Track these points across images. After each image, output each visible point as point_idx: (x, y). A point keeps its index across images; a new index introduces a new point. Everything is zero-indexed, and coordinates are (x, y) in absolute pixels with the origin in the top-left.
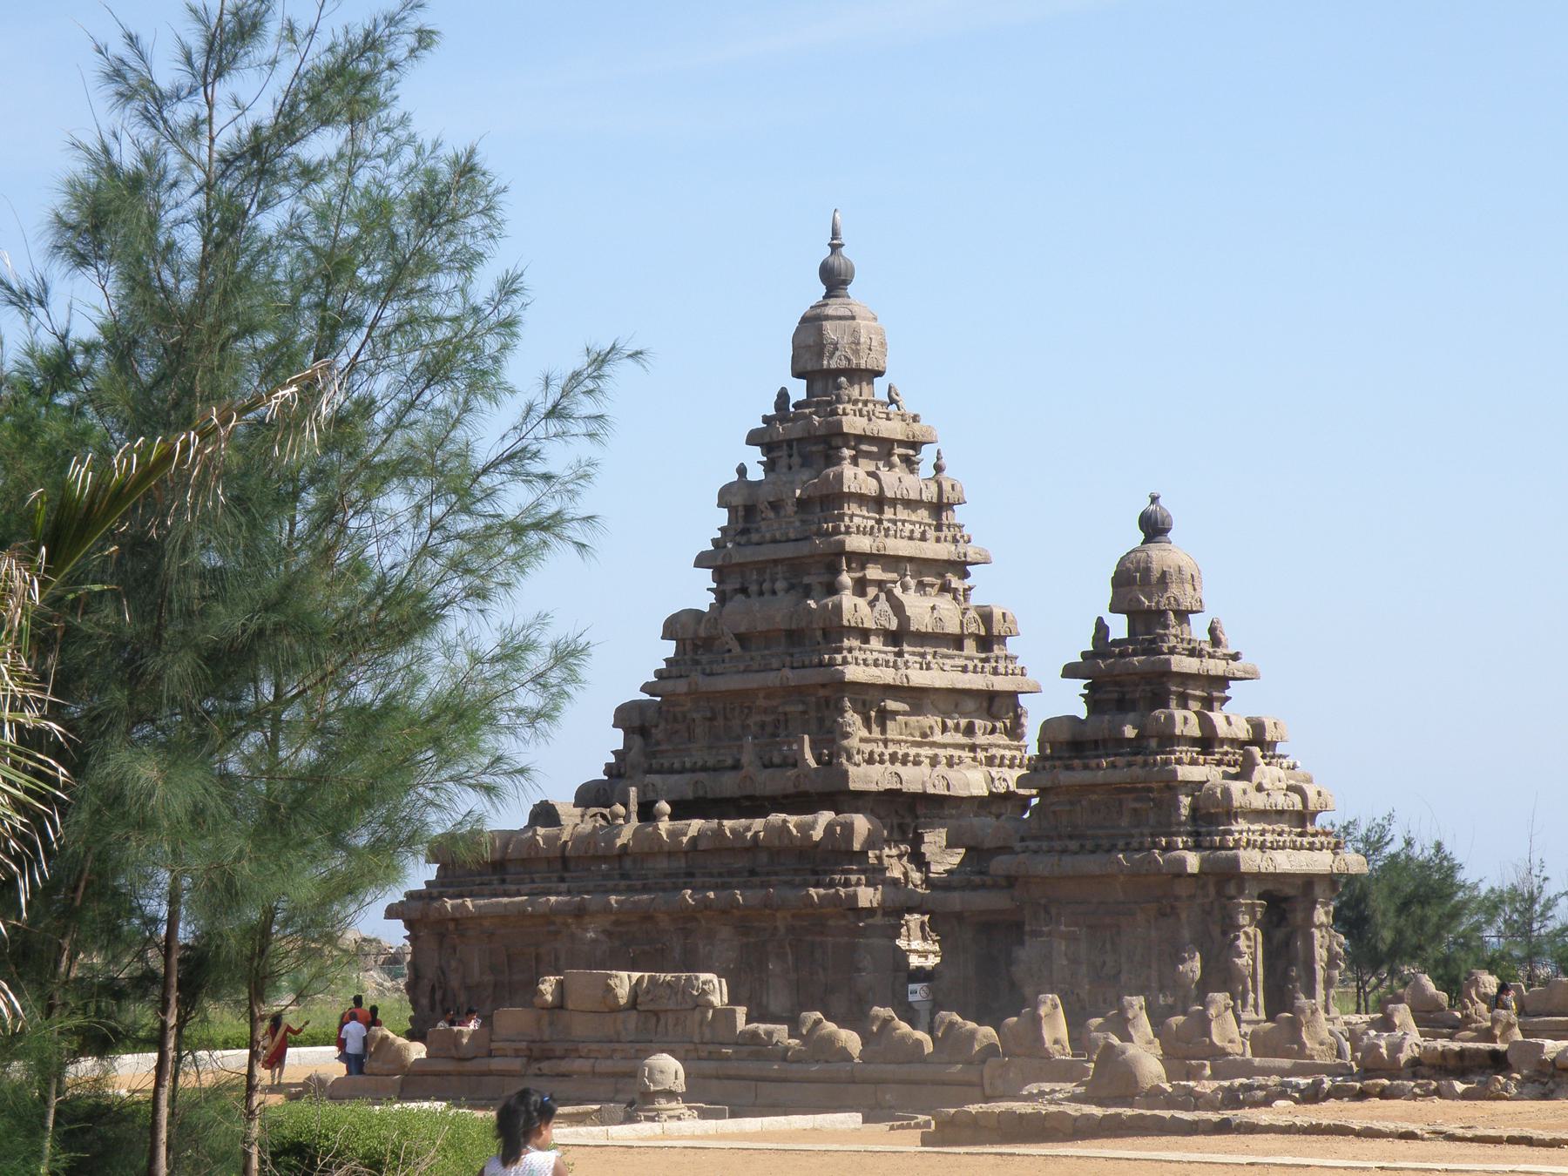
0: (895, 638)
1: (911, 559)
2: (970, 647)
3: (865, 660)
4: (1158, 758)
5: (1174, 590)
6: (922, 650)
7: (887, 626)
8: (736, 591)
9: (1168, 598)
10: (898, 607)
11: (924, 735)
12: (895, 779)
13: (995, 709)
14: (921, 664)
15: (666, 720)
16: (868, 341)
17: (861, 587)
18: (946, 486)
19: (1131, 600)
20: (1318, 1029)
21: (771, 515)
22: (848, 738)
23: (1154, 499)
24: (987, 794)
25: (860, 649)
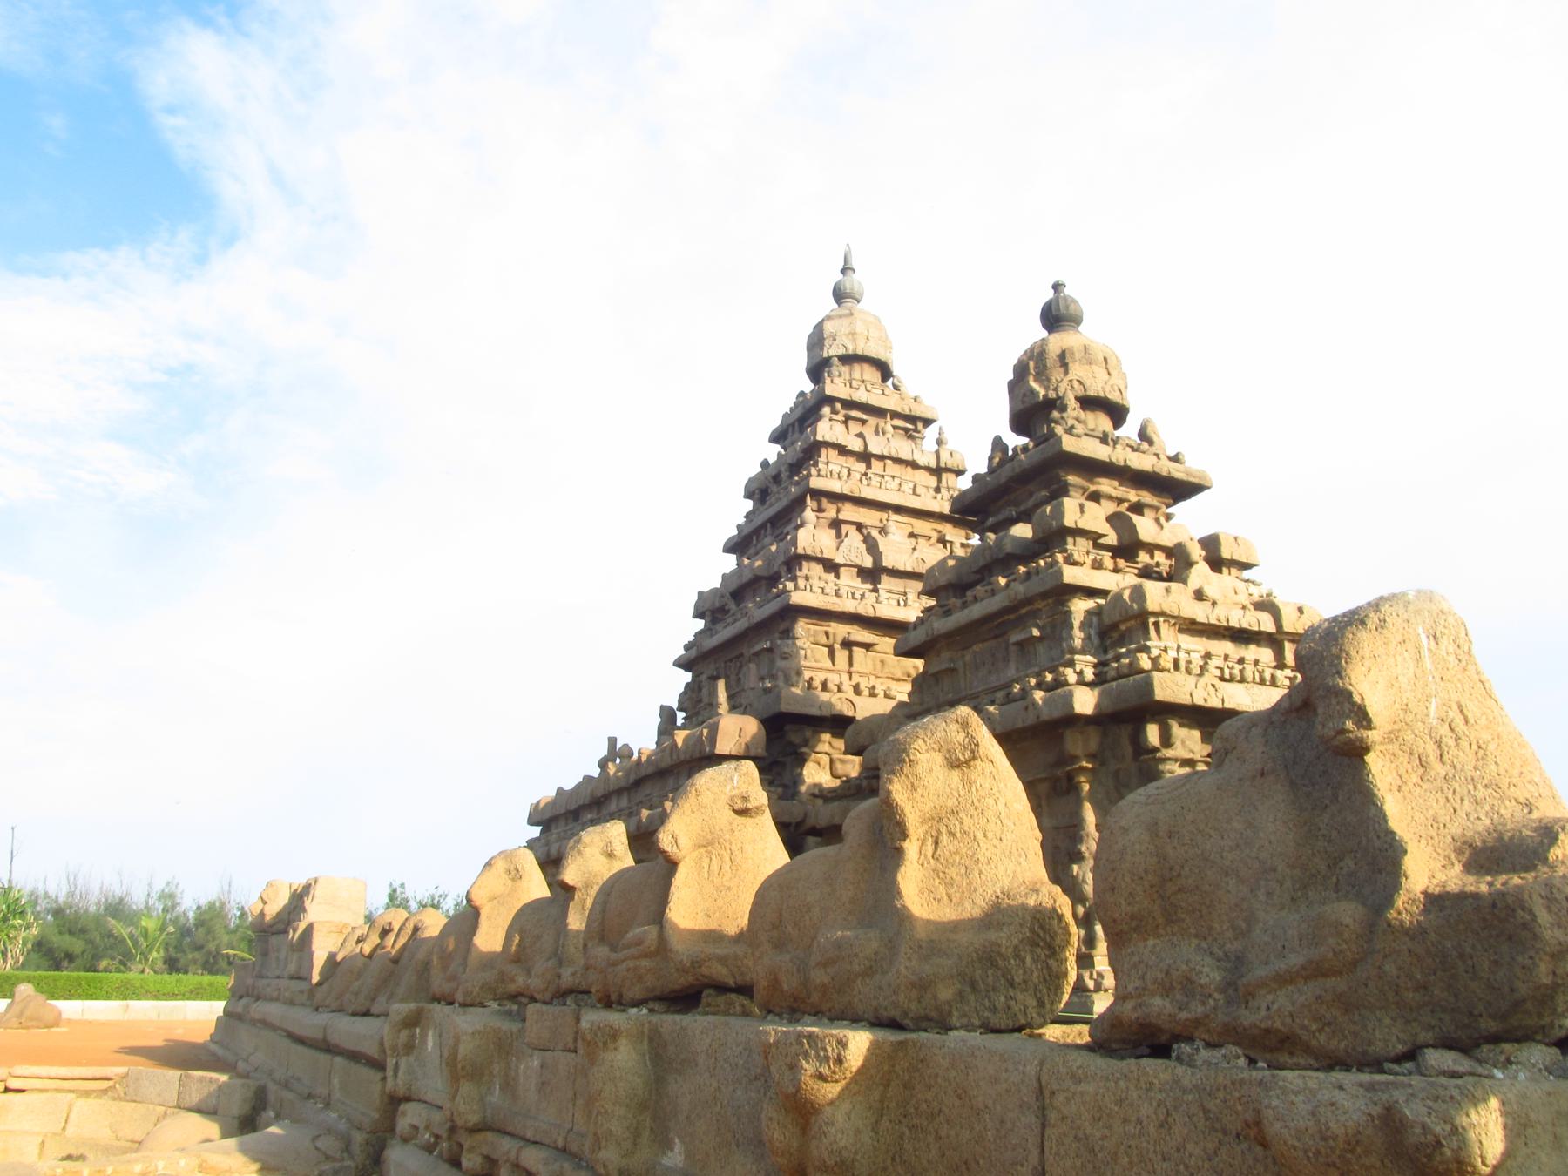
0: (872, 575)
1: (899, 509)
5: (1076, 371)
7: (859, 563)
9: (1071, 381)
10: (872, 547)
14: (899, 602)
15: (693, 691)
16: (866, 332)
17: (836, 524)
18: (945, 457)
19: (1024, 395)
20: (985, 851)
21: (774, 488)
22: (785, 658)
23: (1057, 287)
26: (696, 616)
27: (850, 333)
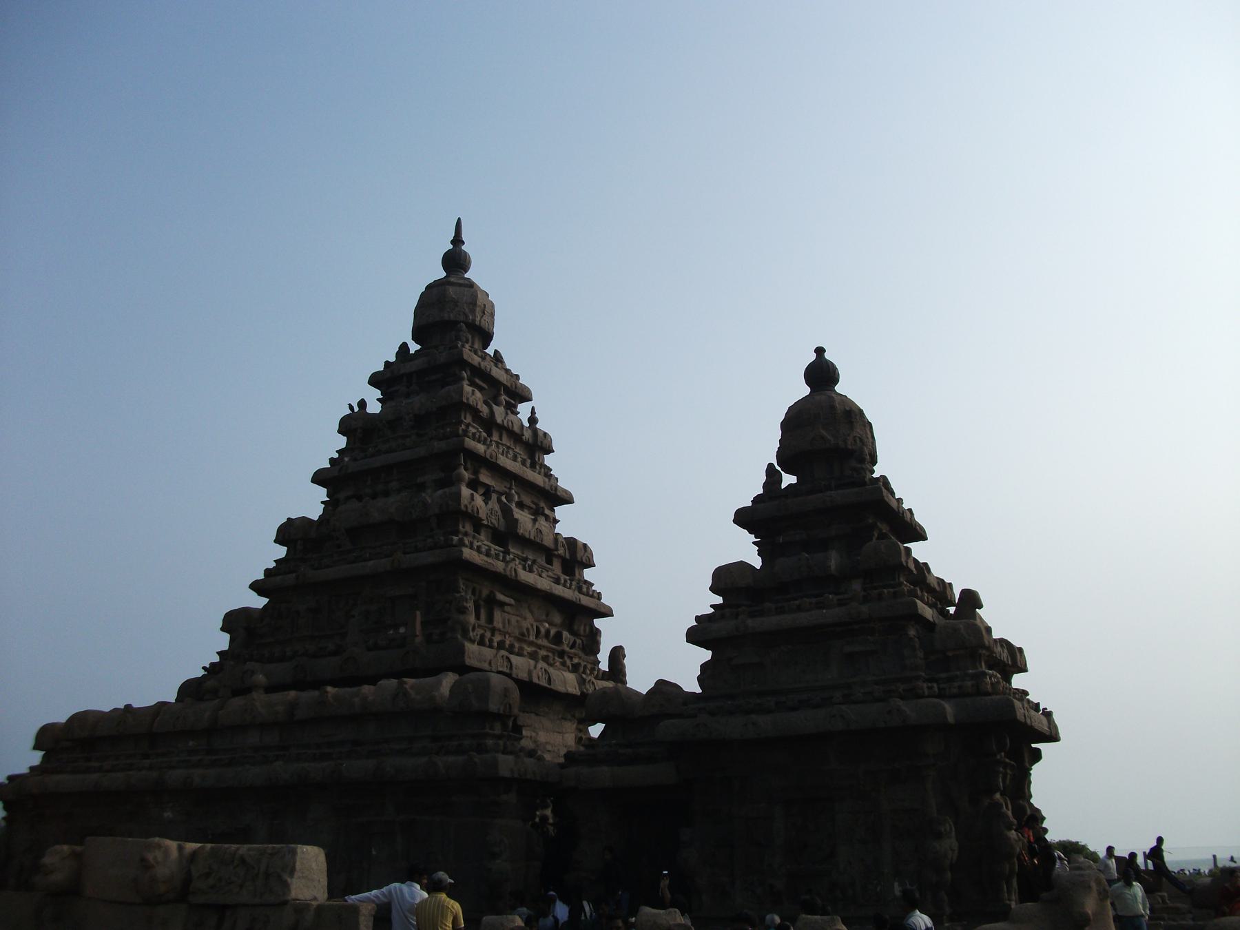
2: (557, 567)
3: (479, 547)
4: (885, 591)
5: (858, 431)
6: (525, 556)
7: (497, 525)
8: (348, 498)
9: (855, 436)
10: (507, 512)
11: (523, 635)
12: (505, 663)
13: (576, 627)
16: (483, 306)
18: (541, 434)
23: (820, 351)
24: (579, 694)
25: (474, 537)
26: (279, 540)
27: (471, 303)
